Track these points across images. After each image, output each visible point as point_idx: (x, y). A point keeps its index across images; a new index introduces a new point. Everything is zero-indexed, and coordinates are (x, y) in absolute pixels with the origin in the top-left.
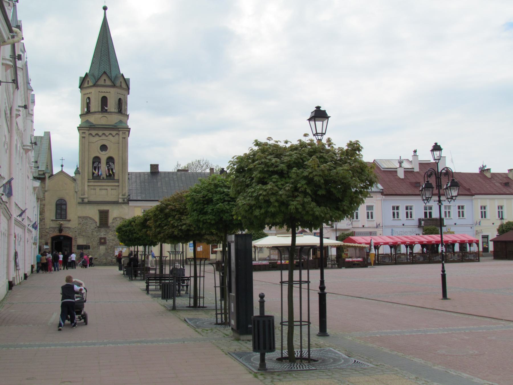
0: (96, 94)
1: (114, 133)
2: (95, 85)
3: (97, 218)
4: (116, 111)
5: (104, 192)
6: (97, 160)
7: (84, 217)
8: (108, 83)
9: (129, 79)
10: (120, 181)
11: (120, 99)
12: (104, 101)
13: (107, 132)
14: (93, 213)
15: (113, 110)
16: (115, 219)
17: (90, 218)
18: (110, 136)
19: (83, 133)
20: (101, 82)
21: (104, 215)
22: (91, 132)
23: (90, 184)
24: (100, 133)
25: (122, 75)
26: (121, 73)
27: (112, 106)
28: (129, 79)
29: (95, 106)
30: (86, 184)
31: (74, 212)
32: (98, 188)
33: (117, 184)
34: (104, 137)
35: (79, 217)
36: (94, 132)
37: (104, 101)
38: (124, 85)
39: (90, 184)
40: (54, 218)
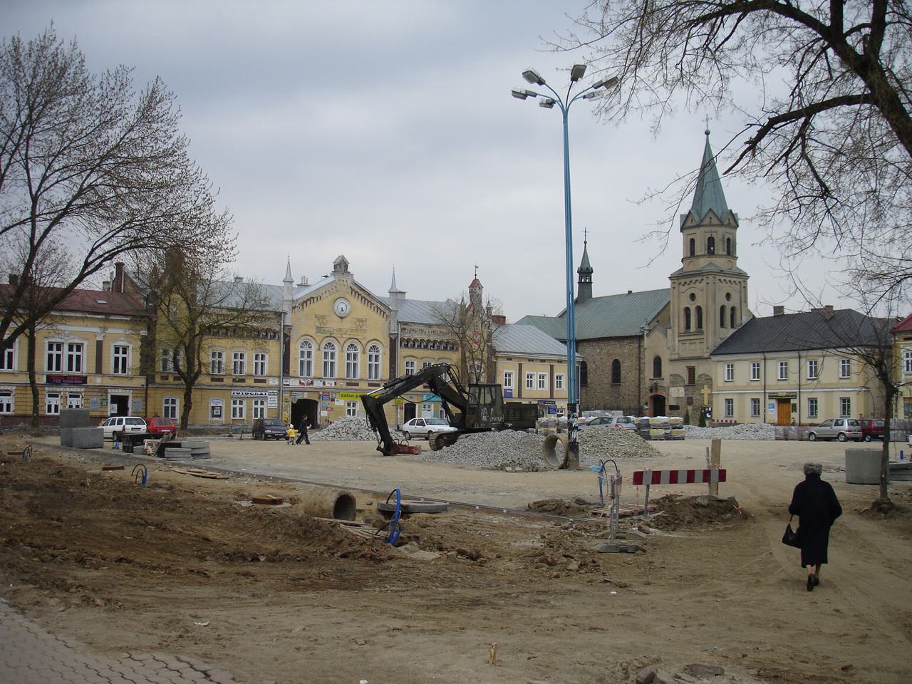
0: (701, 237)
1: (699, 279)
2: (698, 226)
3: (685, 376)
4: (725, 253)
5: (693, 347)
6: (687, 310)
7: (675, 375)
8: (715, 221)
9: (737, 214)
10: (705, 333)
11: (729, 239)
12: (711, 241)
13: (694, 279)
14: (682, 370)
15: (699, 254)
16: (700, 376)
17: (679, 376)
18: (697, 284)
19: (674, 283)
20: (706, 221)
21: (691, 371)
22: (680, 281)
23: (681, 338)
24: (688, 280)
25: (731, 211)
26: (729, 208)
27: (720, 248)
28: (737, 214)
29: (700, 248)
30: (677, 339)
31: (667, 370)
32: (688, 342)
33: (702, 337)
34: (692, 285)
35: (671, 375)
36: (682, 281)
37: (711, 241)
38: (732, 221)
39: (681, 338)
40: (652, 377)
